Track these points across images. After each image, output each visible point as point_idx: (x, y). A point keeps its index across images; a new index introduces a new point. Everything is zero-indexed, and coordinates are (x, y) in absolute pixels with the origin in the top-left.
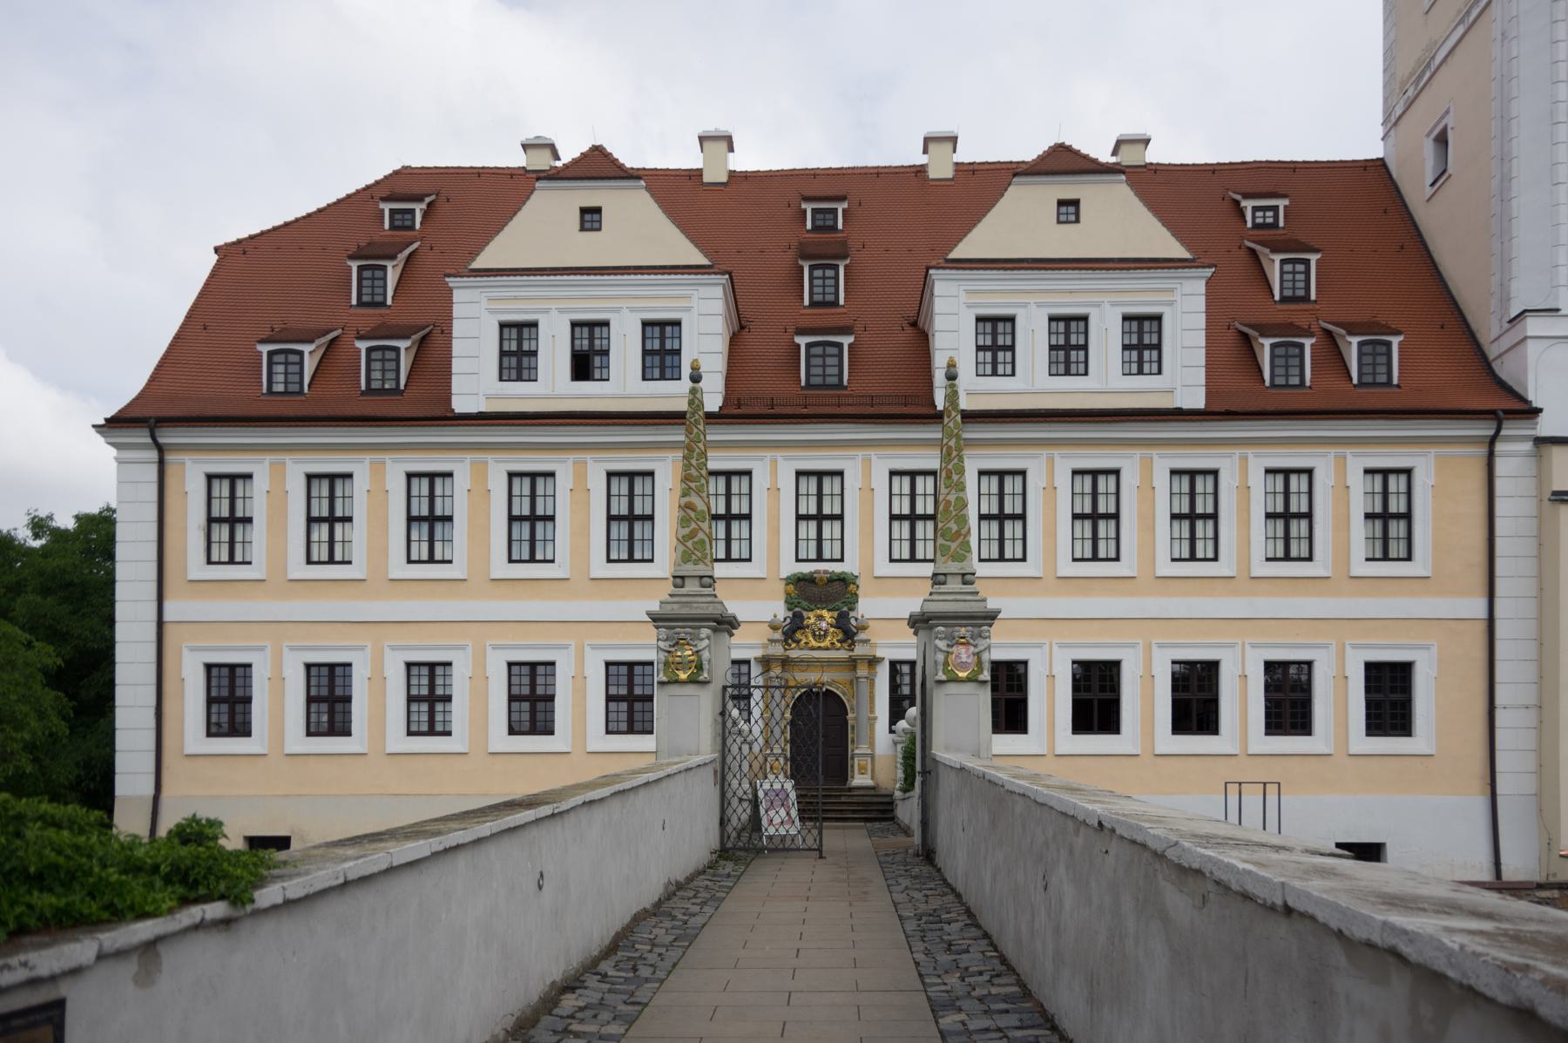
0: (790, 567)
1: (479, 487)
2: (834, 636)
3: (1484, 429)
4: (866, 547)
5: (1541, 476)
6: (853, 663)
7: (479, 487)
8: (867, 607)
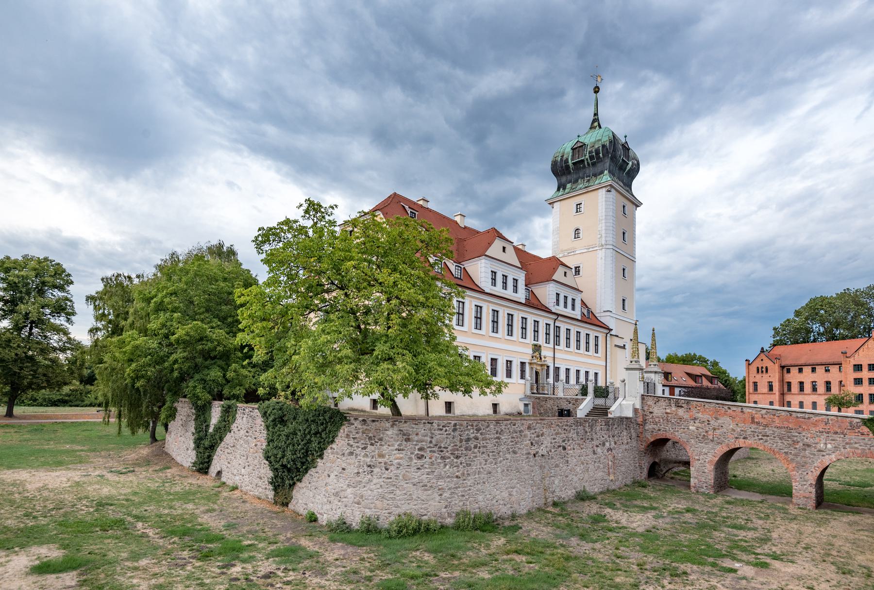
5: (611, 341)
6: (542, 365)
8: (543, 354)
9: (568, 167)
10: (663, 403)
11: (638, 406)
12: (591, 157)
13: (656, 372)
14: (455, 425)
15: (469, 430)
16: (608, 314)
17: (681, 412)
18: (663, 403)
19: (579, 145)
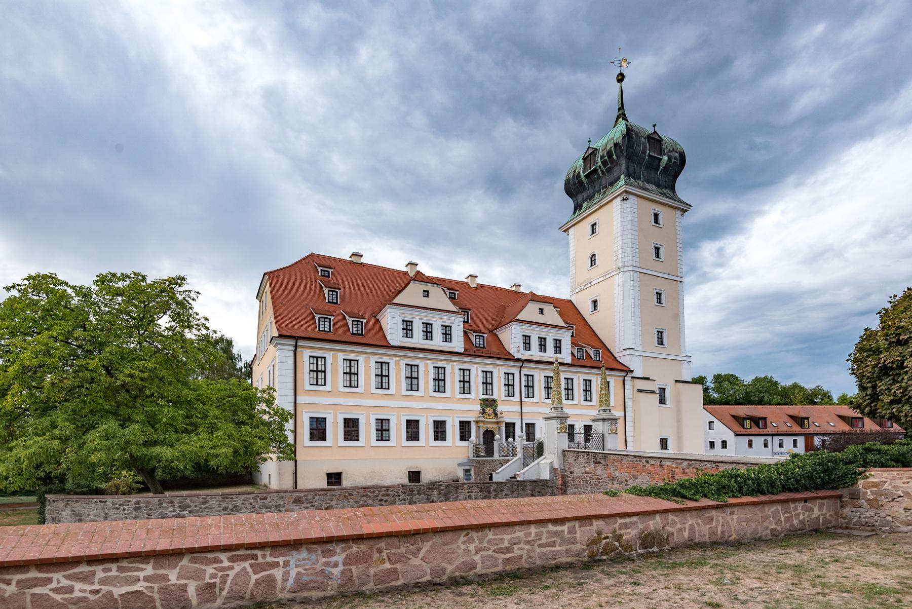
0: (481, 397)
1: (398, 368)
2: (493, 415)
3: (624, 374)
4: (499, 392)
6: (498, 423)
7: (398, 368)
8: (500, 408)
9: (581, 182)
10: (582, 460)
11: (556, 466)
12: (604, 163)
13: (604, 420)
14: (138, 503)
15: (167, 508)
16: (628, 352)
17: (599, 470)
18: (582, 460)
19: (590, 151)
